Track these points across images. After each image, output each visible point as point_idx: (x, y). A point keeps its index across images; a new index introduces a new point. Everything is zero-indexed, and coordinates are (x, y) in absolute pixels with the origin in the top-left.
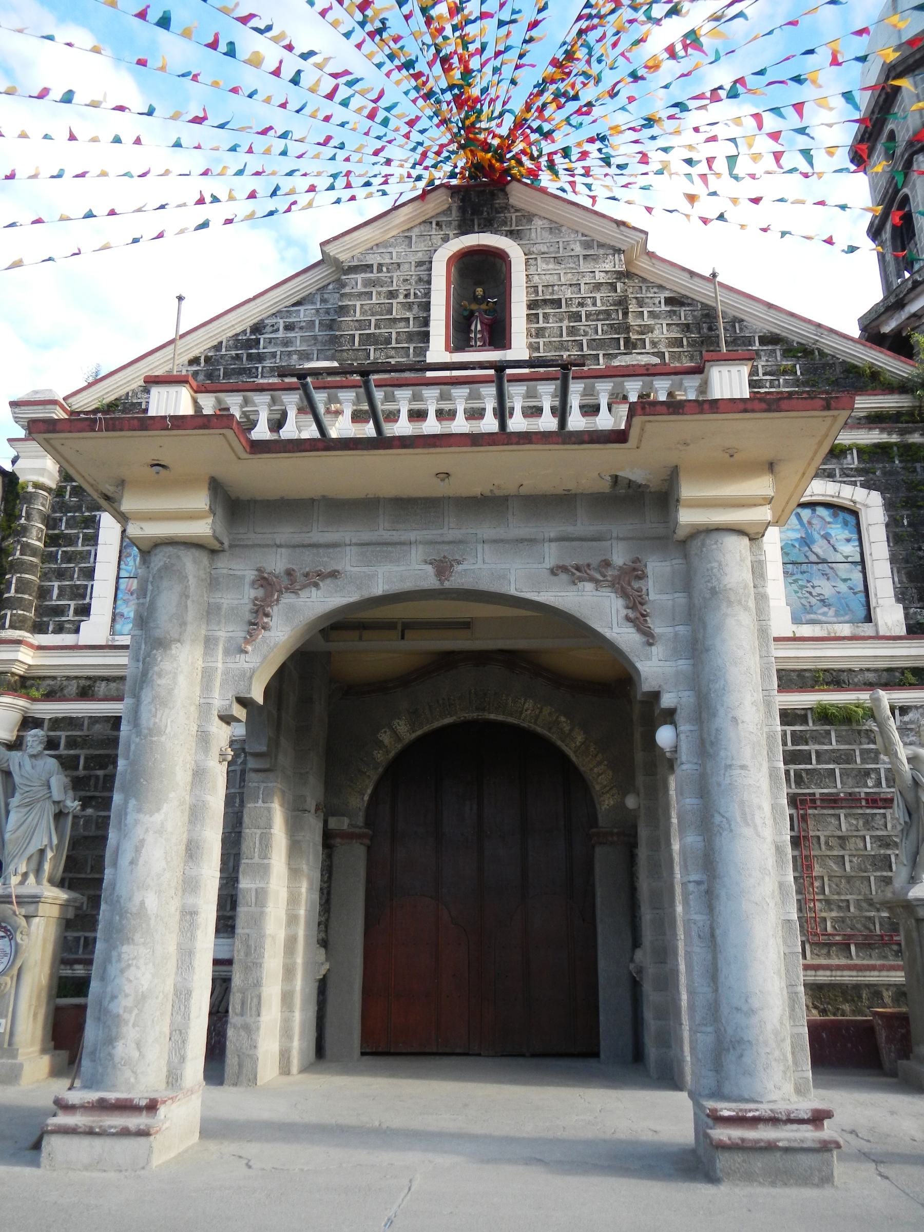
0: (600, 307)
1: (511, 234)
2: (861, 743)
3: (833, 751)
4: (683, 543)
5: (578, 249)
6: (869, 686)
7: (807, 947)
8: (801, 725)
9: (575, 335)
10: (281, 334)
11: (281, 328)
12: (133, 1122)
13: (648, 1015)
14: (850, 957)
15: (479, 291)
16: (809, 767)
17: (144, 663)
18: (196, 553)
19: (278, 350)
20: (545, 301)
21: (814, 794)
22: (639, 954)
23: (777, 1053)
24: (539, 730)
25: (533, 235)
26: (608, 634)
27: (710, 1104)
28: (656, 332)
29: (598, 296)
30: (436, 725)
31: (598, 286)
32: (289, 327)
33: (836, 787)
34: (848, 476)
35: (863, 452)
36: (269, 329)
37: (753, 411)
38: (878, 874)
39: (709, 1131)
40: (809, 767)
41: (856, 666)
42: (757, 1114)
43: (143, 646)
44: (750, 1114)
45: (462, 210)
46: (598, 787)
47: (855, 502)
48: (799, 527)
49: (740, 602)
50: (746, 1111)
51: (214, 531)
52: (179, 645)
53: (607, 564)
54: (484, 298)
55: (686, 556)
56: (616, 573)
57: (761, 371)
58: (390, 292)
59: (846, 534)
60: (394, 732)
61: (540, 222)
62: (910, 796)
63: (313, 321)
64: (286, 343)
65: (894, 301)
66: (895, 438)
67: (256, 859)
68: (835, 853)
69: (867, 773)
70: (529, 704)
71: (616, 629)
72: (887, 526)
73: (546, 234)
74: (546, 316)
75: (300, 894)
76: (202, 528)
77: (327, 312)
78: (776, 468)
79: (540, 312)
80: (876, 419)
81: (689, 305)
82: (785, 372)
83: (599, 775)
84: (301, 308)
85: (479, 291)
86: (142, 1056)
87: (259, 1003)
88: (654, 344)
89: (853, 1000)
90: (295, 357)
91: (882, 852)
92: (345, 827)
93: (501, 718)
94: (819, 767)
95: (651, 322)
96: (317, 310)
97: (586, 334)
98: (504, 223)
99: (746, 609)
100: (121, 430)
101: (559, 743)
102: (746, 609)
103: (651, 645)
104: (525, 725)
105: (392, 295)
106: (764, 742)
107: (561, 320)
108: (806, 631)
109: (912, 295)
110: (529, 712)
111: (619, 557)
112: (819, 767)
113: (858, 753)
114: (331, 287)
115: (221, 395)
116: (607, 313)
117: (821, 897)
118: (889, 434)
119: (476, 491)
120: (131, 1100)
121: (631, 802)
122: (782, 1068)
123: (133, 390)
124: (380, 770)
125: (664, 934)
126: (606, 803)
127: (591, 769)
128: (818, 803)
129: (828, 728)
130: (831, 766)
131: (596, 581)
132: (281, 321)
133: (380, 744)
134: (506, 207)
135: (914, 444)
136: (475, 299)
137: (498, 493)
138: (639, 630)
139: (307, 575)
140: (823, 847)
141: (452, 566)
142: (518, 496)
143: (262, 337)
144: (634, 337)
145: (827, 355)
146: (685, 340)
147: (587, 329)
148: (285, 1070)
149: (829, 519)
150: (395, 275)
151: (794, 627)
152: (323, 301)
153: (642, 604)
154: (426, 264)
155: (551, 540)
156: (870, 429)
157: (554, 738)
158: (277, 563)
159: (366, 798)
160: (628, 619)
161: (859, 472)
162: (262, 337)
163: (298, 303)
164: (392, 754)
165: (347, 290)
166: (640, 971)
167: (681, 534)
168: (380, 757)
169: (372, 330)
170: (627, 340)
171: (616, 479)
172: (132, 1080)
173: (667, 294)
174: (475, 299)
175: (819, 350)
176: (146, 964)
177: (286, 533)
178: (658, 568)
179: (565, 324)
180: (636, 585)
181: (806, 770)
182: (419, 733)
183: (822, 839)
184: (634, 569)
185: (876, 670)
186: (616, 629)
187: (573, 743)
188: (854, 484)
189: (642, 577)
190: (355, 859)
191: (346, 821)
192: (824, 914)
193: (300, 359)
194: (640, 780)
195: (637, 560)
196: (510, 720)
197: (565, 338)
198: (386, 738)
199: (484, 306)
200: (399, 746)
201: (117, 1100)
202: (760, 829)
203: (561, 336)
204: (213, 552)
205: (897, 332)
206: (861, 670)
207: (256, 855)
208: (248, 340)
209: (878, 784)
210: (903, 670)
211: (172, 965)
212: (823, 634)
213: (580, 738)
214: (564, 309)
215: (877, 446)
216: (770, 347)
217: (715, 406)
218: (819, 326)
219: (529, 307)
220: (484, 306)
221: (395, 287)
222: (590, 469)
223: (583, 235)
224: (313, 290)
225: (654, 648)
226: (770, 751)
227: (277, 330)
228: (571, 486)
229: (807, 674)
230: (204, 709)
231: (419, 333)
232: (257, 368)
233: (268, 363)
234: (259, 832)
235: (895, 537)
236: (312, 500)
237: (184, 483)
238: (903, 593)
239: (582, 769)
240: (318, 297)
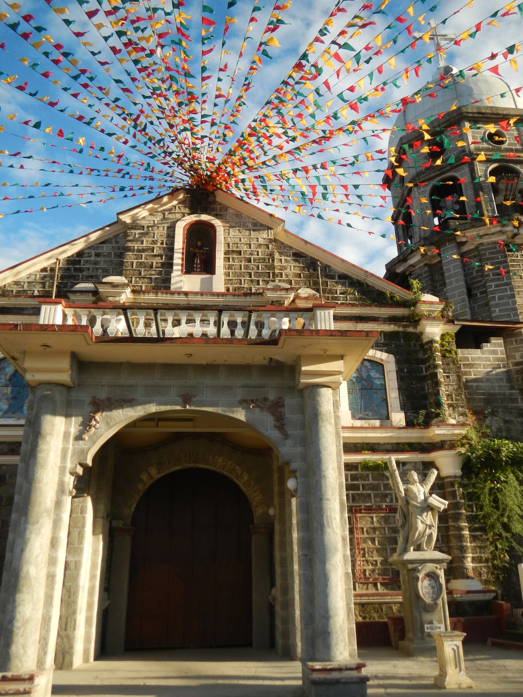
0: (260, 255)
1: (217, 216)
2: (383, 480)
4: (301, 391)
5: (250, 226)
6: (388, 451)
7: (357, 584)
9: (247, 269)
10: (93, 258)
11: (93, 255)
12: (21, 687)
13: (278, 623)
14: (377, 589)
15: (199, 243)
16: (359, 492)
17: (31, 445)
18: (61, 388)
19: (91, 266)
21: (360, 506)
22: (274, 591)
23: (341, 637)
24: (225, 473)
25: (228, 217)
26: (266, 433)
27: (310, 664)
28: (288, 270)
29: (260, 250)
30: (172, 470)
31: (260, 245)
32: (97, 255)
34: (379, 346)
35: (387, 335)
36: (86, 255)
37: (335, 336)
38: (391, 546)
39: (310, 676)
40: (359, 492)
41: (382, 442)
42: (332, 667)
43: (31, 437)
44: (329, 667)
45: (192, 201)
46: (254, 504)
47: (382, 360)
49: (327, 420)
50: (327, 666)
51: (72, 379)
52: (50, 436)
53: (266, 399)
54: (201, 248)
55: (302, 397)
56: (270, 404)
57: (338, 292)
58: (153, 241)
59: (378, 375)
60: (149, 474)
61: (231, 211)
62: (405, 510)
63: (110, 253)
64: (96, 263)
65: (402, 258)
66: (401, 329)
67: (76, 545)
68: (371, 536)
69: (386, 496)
70: (220, 460)
71: (270, 432)
72: (397, 372)
73: (234, 217)
74: (233, 259)
75: (97, 563)
76: (65, 377)
77: (119, 248)
78: (345, 358)
79: (230, 256)
80: (392, 320)
81: (304, 257)
82: (350, 294)
83: (255, 497)
84: (105, 245)
85: (199, 243)
86: (25, 652)
87: (75, 623)
88: (287, 276)
89: (378, 611)
90: (100, 271)
91: (393, 535)
92: (121, 526)
93: (205, 467)
94: (364, 492)
95: (286, 264)
96: (113, 247)
97: (253, 269)
98: (213, 210)
99: (330, 423)
100: (31, 330)
101: (235, 480)
102: (330, 423)
103: (286, 439)
104: (218, 470)
105: (154, 242)
106: (337, 487)
107: (241, 261)
108: (358, 423)
109: (410, 256)
110: (220, 464)
111: (272, 396)
112: (364, 492)
113: (382, 485)
114: (121, 235)
115: (78, 310)
117: (364, 559)
118: (399, 327)
119: (204, 362)
120: (20, 676)
121: (271, 512)
122: (343, 644)
123: (9, 284)
124: (141, 494)
125: (287, 580)
126: (258, 512)
127: (251, 494)
129: (368, 472)
130: (369, 492)
131: (261, 408)
132: (93, 251)
133: (141, 480)
134: (214, 202)
135: (410, 332)
136: (196, 247)
137: (214, 363)
138: (280, 432)
139: (117, 401)
140: (365, 533)
141: (191, 398)
142: (224, 365)
143: (82, 259)
144: (277, 271)
145: (370, 286)
147: (254, 267)
148: (86, 660)
149: (370, 367)
150: (156, 232)
151: (352, 421)
152: (117, 242)
153: (282, 419)
154: (172, 229)
155: (239, 387)
156: (390, 324)
157: (233, 477)
158: (103, 394)
159: (133, 509)
160: (275, 426)
161: (384, 345)
162: (82, 259)
163: (103, 243)
164: (147, 486)
165: (130, 238)
166: (274, 599)
167: (300, 387)
168: (141, 488)
169: (143, 260)
170: (274, 274)
171: (271, 359)
172: (20, 665)
173: (294, 251)
174: (196, 247)
175: (366, 283)
176: (28, 603)
177: (108, 379)
178: (290, 402)
179: (243, 263)
180: (279, 410)
181: (358, 494)
182: (162, 475)
183: (365, 529)
184: (279, 402)
185: (391, 444)
186: (270, 432)
187: (243, 480)
188: (381, 350)
189: (283, 406)
190: (126, 543)
191: (122, 522)
192: (365, 568)
193: (103, 272)
194: (276, 500)
195: (281, 398)
196: (211, 468)
197: (243, 270)
198: (144, 477)
199: (201, 251)
200: (152, 482)
201: (12, 676)
202: (335, 529)
203: (241, 269)
204: (69, 388)
205: (403, 273)
206: (384, 444)
207: (76, 542)
208: (75, 260)
209: (392, 501)
210: (403, 444)
211: (41, 604)
212: (366, 425)
213: (246, 477)
214: (242, 256)
215: (392, 333)
216: (343, 281)
217: (318, 332)
218: (366, 272)
220: (201, 251)
221: (155, 239)
222: (260, 355)
223: (253, 219)
224: (111, 236)
225: (287, 441)
226: (340, 491)
227: (91, 256)
228: (250, 362)
229: (359, 445)
230: (62, 470)
231: (168, 263)
232: (79, 276)
233: (85, 273)
234: (78, 530)
235: (400, 378)
236: (121, 364)
237: (58, 354)
238: (404, 406)
239: (247, 494)
240: (114, 240)
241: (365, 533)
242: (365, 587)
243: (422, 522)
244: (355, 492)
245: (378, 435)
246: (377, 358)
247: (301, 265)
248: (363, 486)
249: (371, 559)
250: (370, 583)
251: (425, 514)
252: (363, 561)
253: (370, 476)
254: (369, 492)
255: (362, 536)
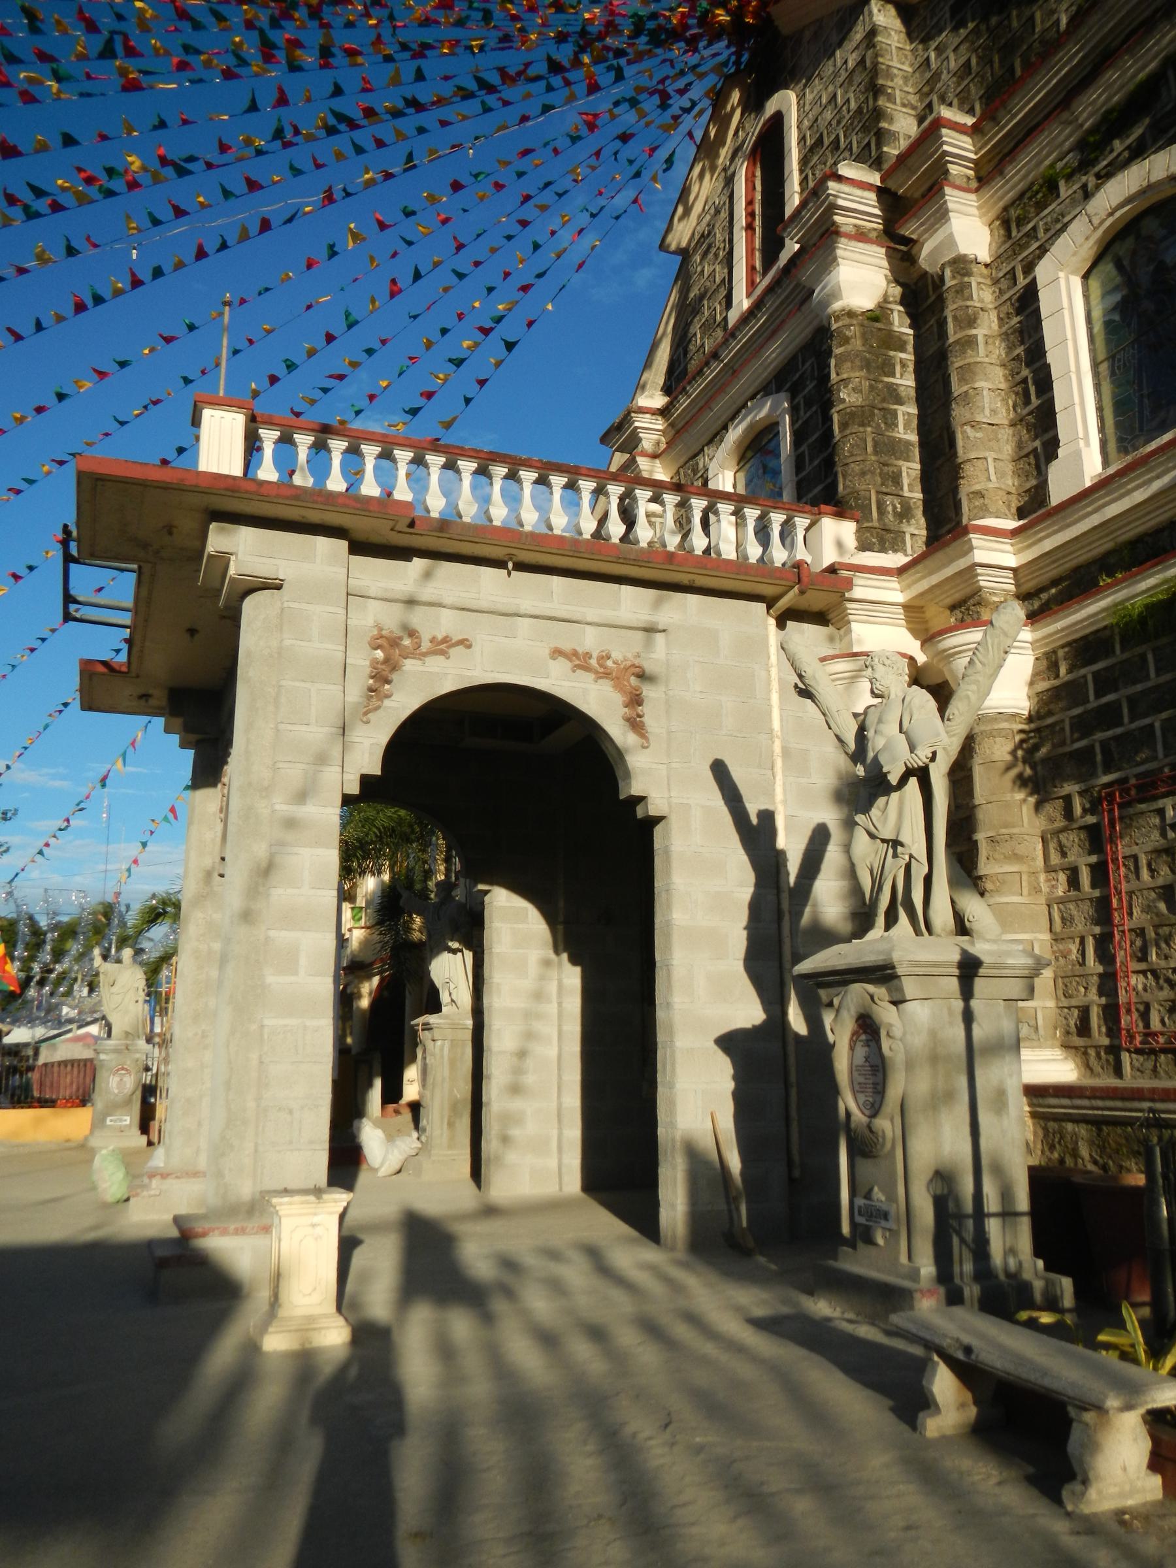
3: (1157, 687)
8: (1107, 657)
14: (1118, 1072)
16: (1119, 731)
20: (812, 150)
28: (945, 76)
33: (1155, 758)
48: (1118, 280)
116: (859, 110)
117: (1143, 966)
128: (1133, 792)
129: (1139, 650)
130: (1147, 721)
140: (1145, 874)
146: (974, 61)
181: (1116, 738)
183: (1143, 861)
192: (1147, 997)
214: (826, 142)
219: (801, 171)
223: (838, 11)
241: (1145, 874)
242: (1149, 1065)
243: (872, 836)
244: (1110, 733)
245: (1139, 496)
246: (1160, 183)
247: (971, 25)
248: (1132, 701)
249: (1163, 963)
250: (1164, 1051)
251: (881, 801)
252: (1144, 973)
253: (1150, 657)
254: (1147, 721)
255: (1134, 884)
